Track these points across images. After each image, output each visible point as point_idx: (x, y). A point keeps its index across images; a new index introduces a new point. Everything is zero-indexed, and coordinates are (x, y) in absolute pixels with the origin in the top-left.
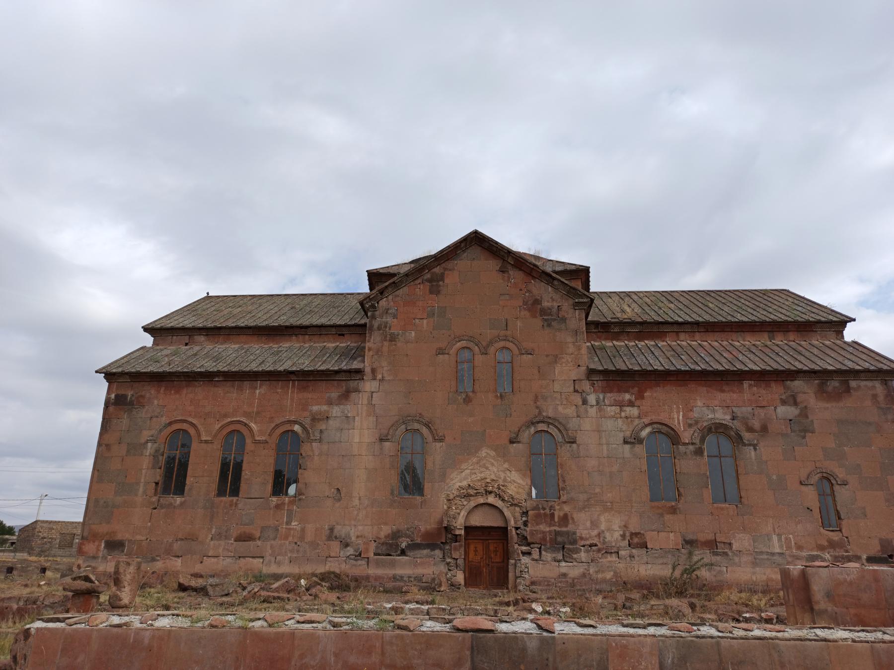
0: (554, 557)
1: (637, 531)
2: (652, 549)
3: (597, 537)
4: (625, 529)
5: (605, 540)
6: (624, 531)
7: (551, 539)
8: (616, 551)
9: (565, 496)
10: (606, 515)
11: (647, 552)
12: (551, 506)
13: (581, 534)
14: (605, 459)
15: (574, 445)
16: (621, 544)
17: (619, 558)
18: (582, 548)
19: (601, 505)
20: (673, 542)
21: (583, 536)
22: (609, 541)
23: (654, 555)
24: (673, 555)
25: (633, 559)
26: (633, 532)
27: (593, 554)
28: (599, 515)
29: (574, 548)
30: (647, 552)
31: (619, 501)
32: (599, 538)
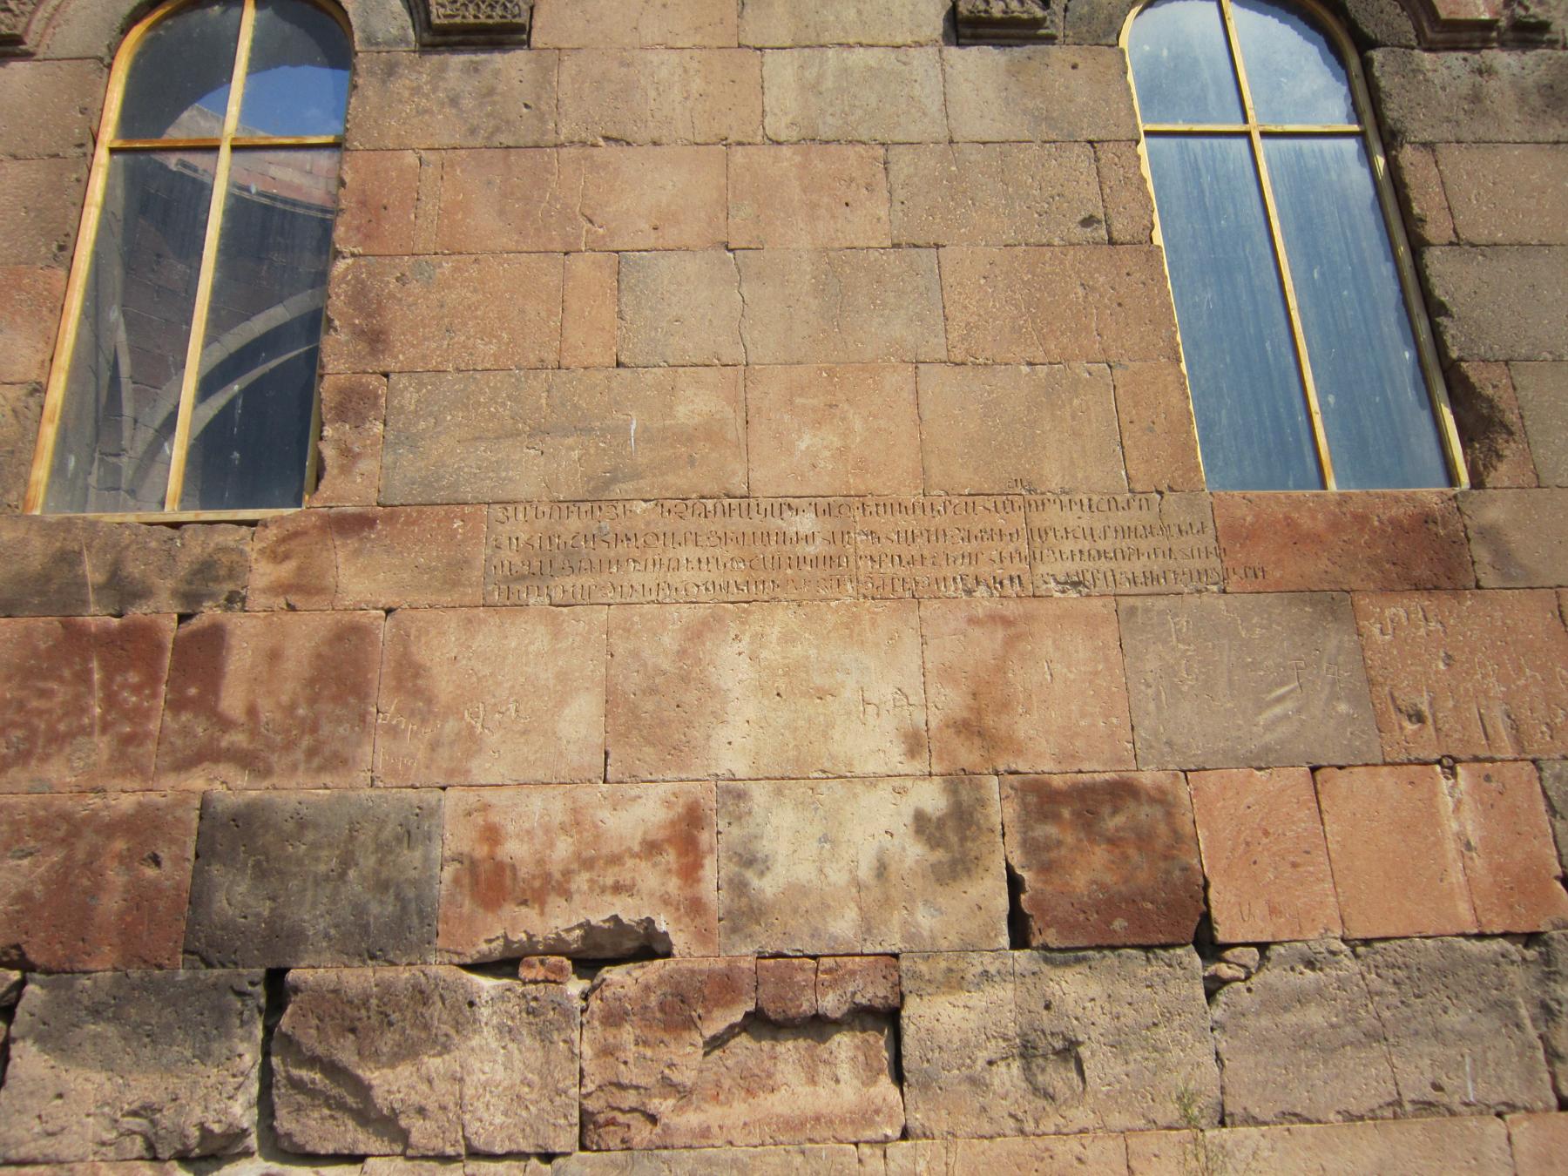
0: (143, 1111)
1: (1098, 771)
2: (1263, 947)
3: (670, 857)
4: (968, 756)
5: (755, 882)
6: (957, 780)
7: (141, 899)
8: (874, 992)
9: (365, 465)
10: (774, 633)
11: (1214, 987)
12: (206, 570)
13: (492, 835)
14: (786, 151)
15: (510, 64)
16: (925, 920)
17: (899, 1077)
18: (486, 984)
19: (724, 539)
20: (1479, 862)
21: (514, 849)
22: (803, 891)
23: (1290, 1019)
24: (1496, 1005)
25: (1057, 1077)
26: (1057, 781)
27: (607, 1051)
28: (696, 633)
29: (387, 989)
30: (1214, 987)
31: (909, 496)
32: (690, 871)
